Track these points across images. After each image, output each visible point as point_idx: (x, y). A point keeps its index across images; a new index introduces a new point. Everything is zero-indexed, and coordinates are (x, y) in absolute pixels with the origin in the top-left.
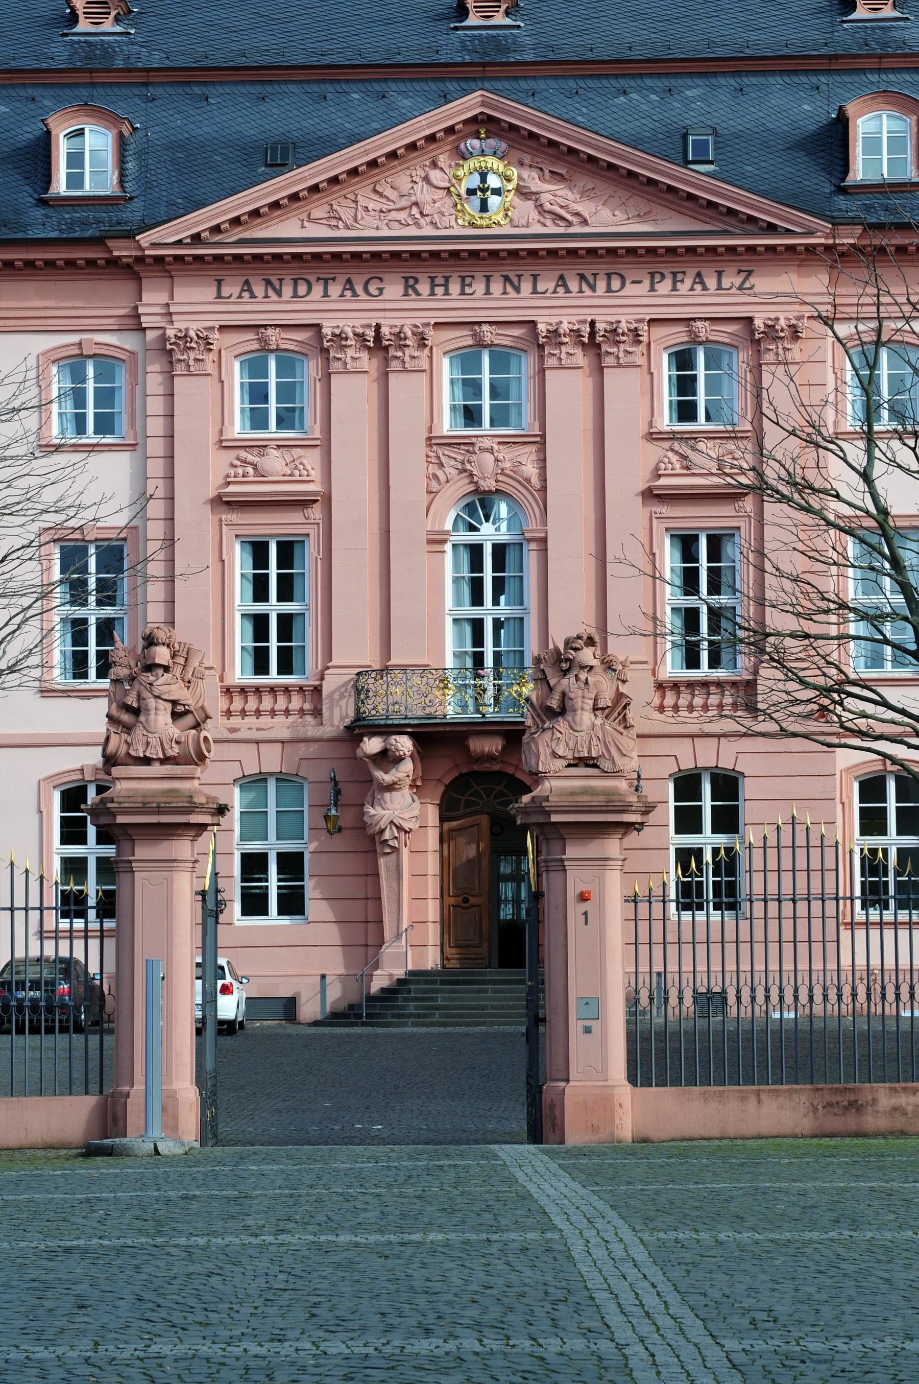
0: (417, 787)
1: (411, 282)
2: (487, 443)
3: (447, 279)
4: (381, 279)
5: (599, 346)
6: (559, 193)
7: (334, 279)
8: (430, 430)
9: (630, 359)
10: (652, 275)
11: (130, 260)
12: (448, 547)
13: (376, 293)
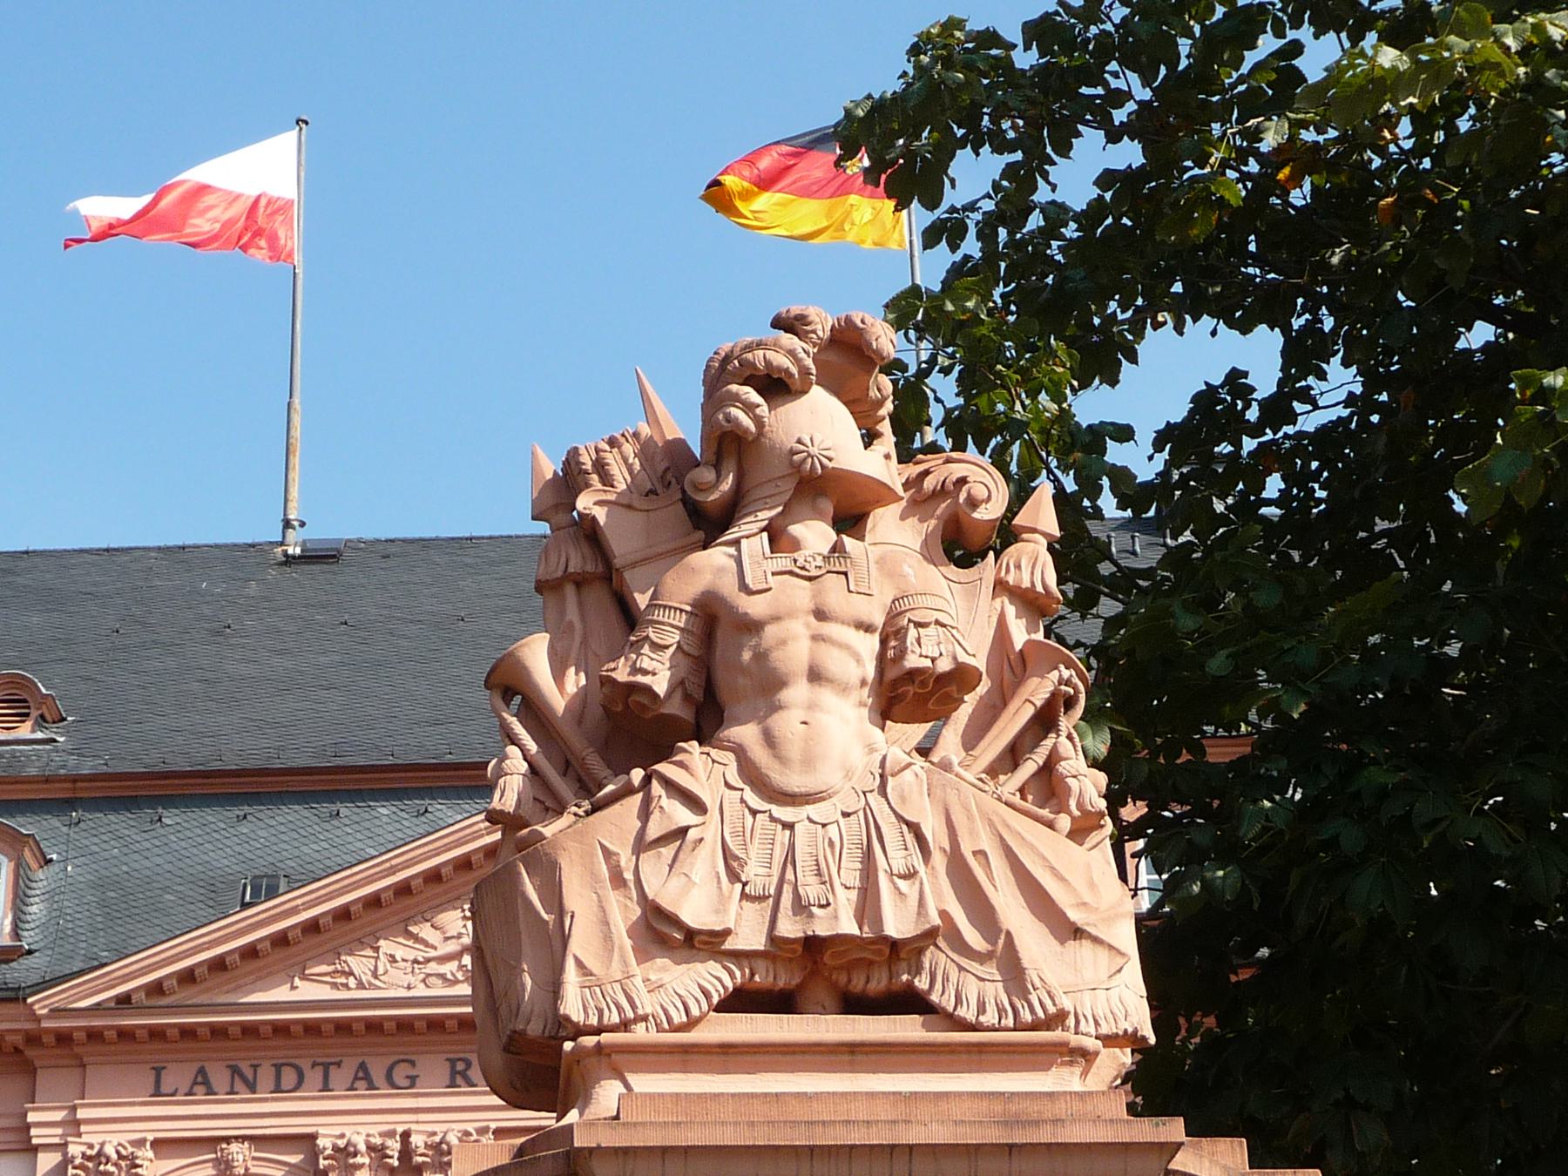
1: (460, 1066)
4: (413, 1063)
7: (338, 1064)
11: (18, 1039)
13: (407, 1083)
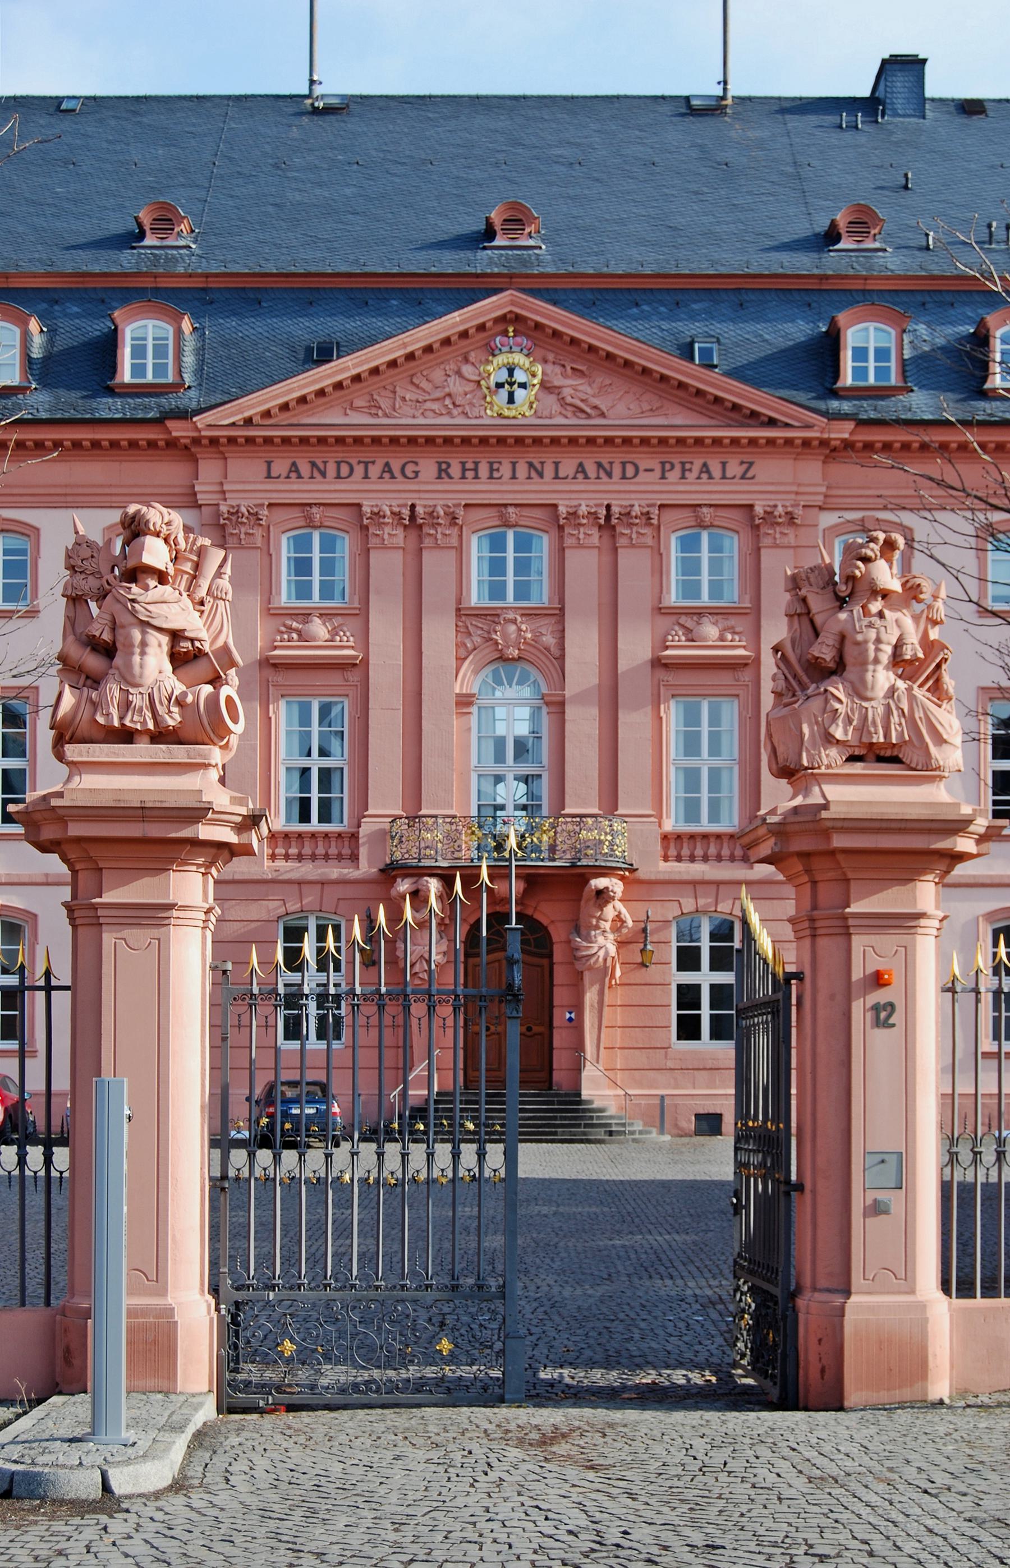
1: (444, 466)
2: (511, 615)
3: (476, 464)
4: (416, 464)
5: (614, 527)
6: (581, 388)
7: (373, 463)
8: (459, 601)
9: (642, 540)
10: (663, 464)
11: (187, 441)
12: (474, 709)
13: (410, 475)
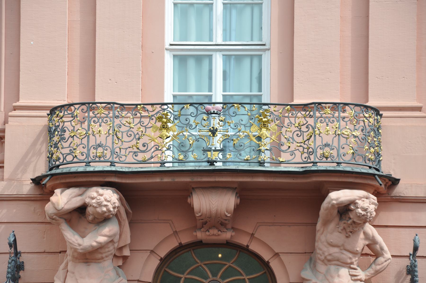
0: (125, 258)
